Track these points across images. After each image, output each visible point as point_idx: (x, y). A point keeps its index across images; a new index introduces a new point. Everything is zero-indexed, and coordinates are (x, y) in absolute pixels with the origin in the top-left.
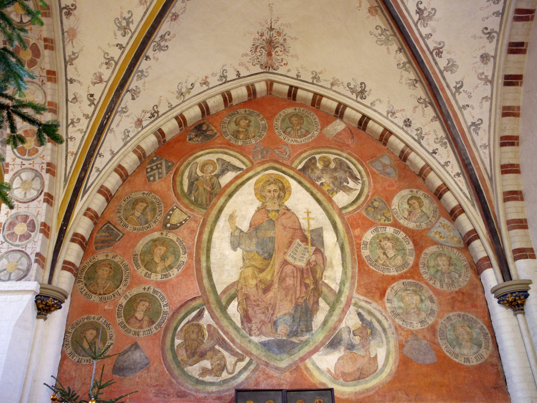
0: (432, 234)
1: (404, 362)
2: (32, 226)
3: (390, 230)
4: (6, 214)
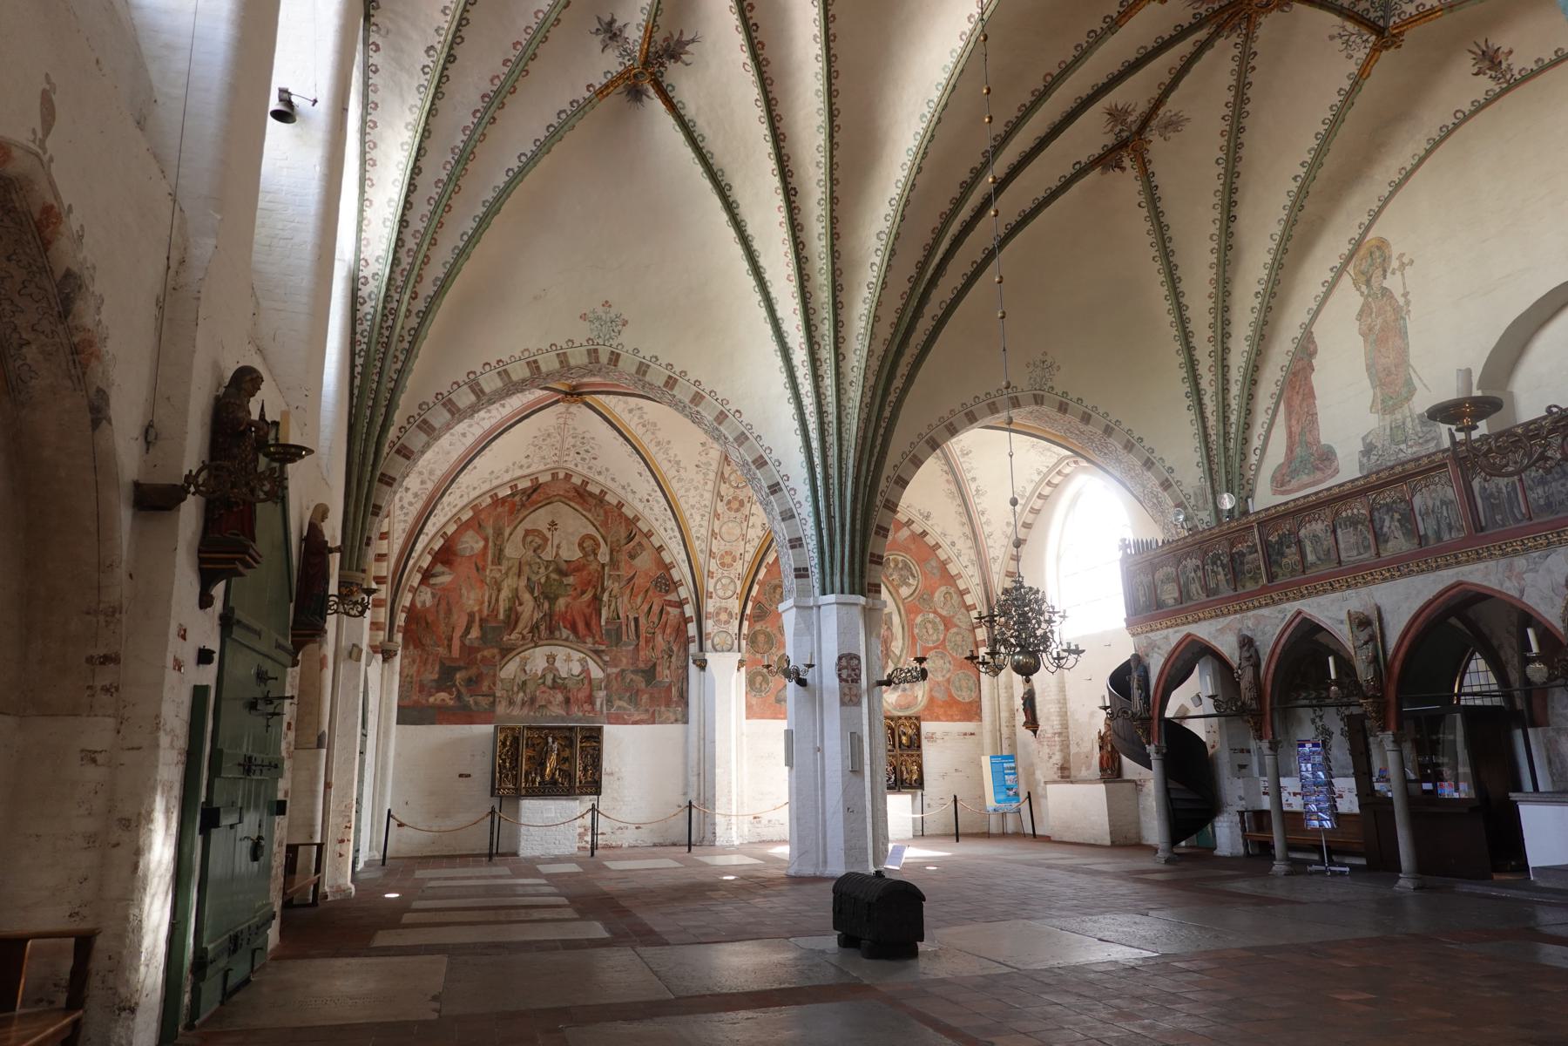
0: (955, 620)
1: (932, 700)
2: (730, 615)
3: (932, 616)
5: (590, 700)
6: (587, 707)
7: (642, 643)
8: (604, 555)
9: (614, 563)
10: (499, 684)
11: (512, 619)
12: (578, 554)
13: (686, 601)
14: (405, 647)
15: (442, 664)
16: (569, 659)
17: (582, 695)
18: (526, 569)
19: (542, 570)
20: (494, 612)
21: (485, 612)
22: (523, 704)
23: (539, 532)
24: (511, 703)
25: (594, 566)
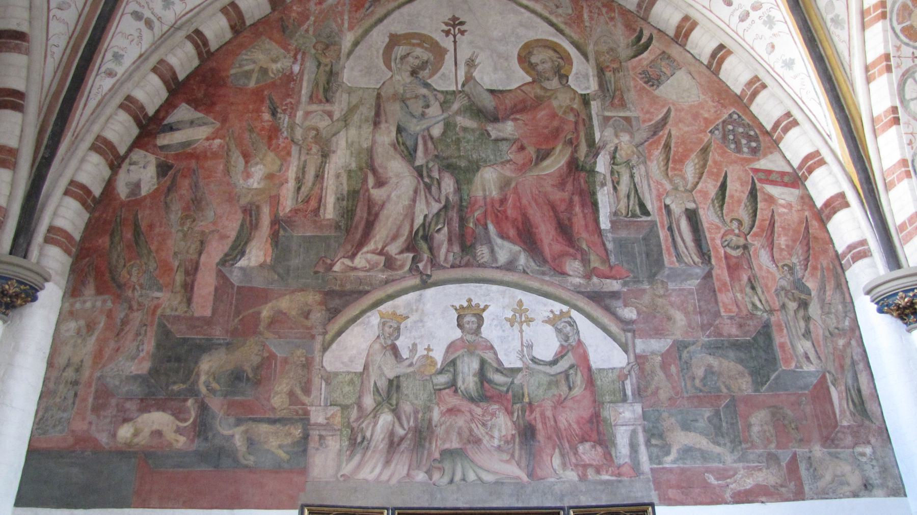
4: (909, 144)
5: (596, 431)
6: (588, 453)
7: (720, 272)
8: (583, 78)
9: (611, 93)
10: (320, 389)
11: (358, 219)
12: (520, 77)
13: (814, 161)
14: (73, 291)
15: (165, 334)
16: (520, 318)
17: (569, 418)
18: (394, 110)
19: (434, 110)
20: (310, 206)
21: (288, 203)
22: (393, 444)
23: (424, 40)
24: (356, 443)
25: (561, 101)
